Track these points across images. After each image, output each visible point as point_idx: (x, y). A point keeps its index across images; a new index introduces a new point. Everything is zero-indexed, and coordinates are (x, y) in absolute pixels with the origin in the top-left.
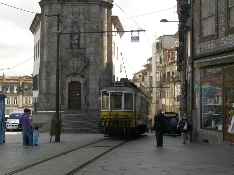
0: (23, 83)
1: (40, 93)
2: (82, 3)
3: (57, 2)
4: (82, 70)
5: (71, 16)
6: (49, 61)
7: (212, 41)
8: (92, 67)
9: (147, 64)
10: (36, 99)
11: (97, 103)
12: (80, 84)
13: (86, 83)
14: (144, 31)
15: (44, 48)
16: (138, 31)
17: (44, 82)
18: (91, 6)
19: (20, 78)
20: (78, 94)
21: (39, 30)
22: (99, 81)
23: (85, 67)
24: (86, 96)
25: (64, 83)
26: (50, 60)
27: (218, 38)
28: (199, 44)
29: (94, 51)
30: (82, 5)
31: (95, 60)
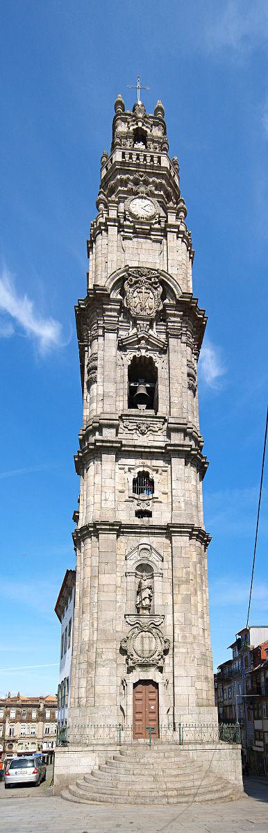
3: (108, 527)
6: (93, 641)
11: (194, 724)
12: (156, 685)
17: (83, 683)
20: (152, 707)
23: (166, 652)
31: (184, 637)
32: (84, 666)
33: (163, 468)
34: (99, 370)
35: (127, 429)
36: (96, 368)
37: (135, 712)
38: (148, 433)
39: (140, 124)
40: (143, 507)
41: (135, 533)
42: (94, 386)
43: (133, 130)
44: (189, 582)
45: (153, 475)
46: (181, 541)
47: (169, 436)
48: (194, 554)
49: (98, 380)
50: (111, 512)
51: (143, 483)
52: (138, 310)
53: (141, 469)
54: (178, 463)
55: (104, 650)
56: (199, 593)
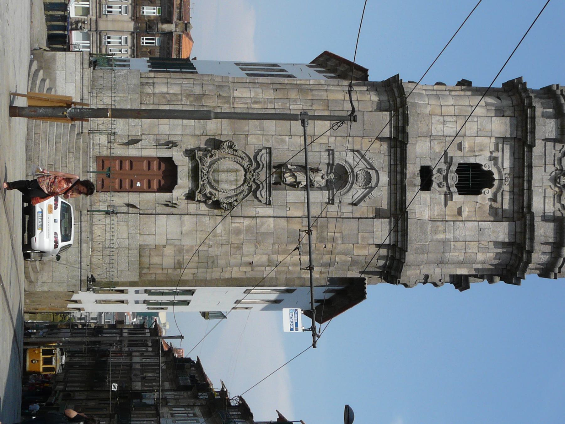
0: (171, 33)
2: (398, 195)
3: (400, 125)
4: (209, 195)
14: (314, 346)
18: (388, 220)
19: (186, 24)
20: (138, 184)
25: (170, 145)
29: (263, 229)
30: (393, 195)
31: (238, 232)
32: (198, 90)
35: (560, 155)
37: (132, 161)
38: (557, 189)
40: (436, 178)
41: (396, 165)
44: (321, 242)
45: (488, 193)
46: (382, 231)
47: (545, 218)
50: (423, 129)
51: (473, 179)
53: (496, 176)
54: (502, 231)
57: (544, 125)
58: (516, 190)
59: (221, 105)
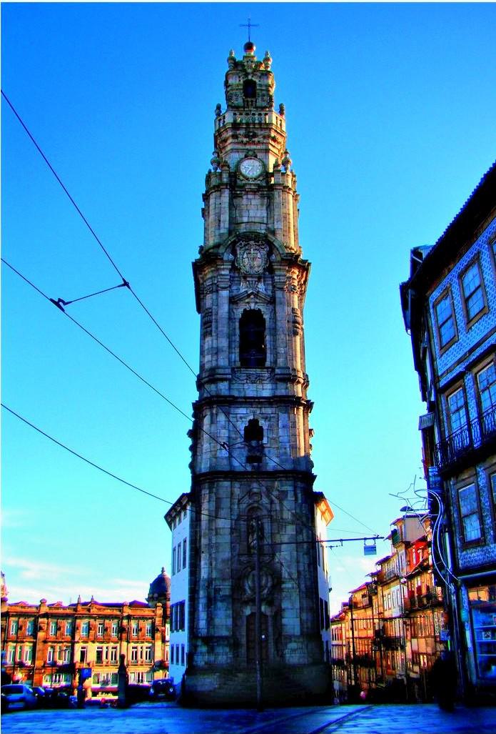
1: (193, 634)
5: (246, 500)
6: (212, 579)
7: (479, 549)
8: (288, 585)
9: (374, 571)
10: (178, 648)
13: (279, 614)
15: (203, 555)
16: (374, 539)
17: (203, 615)
21: (185, 522)
22: (298, 611)
23: (273, 587)
24: (277, 639)
26: (214, 577)
27: (485, 545)
28: (462, 552)
29: (289, 559)
31: (290, 574)
33: (272, 415)
34: (214, 325)
36: (211, 322)
39: (250, 77)
42: (208, 339)
43: (244, 82)
45: (262, 423)
48: (299, 495)
49: (214, 334)
50: (225, 462)
52: (247, 268)
53: (251, 417)
55: (221, 587)
56: (304, 531)
57: (221, 390)
58: (259, 406)
59: (213, 587)
